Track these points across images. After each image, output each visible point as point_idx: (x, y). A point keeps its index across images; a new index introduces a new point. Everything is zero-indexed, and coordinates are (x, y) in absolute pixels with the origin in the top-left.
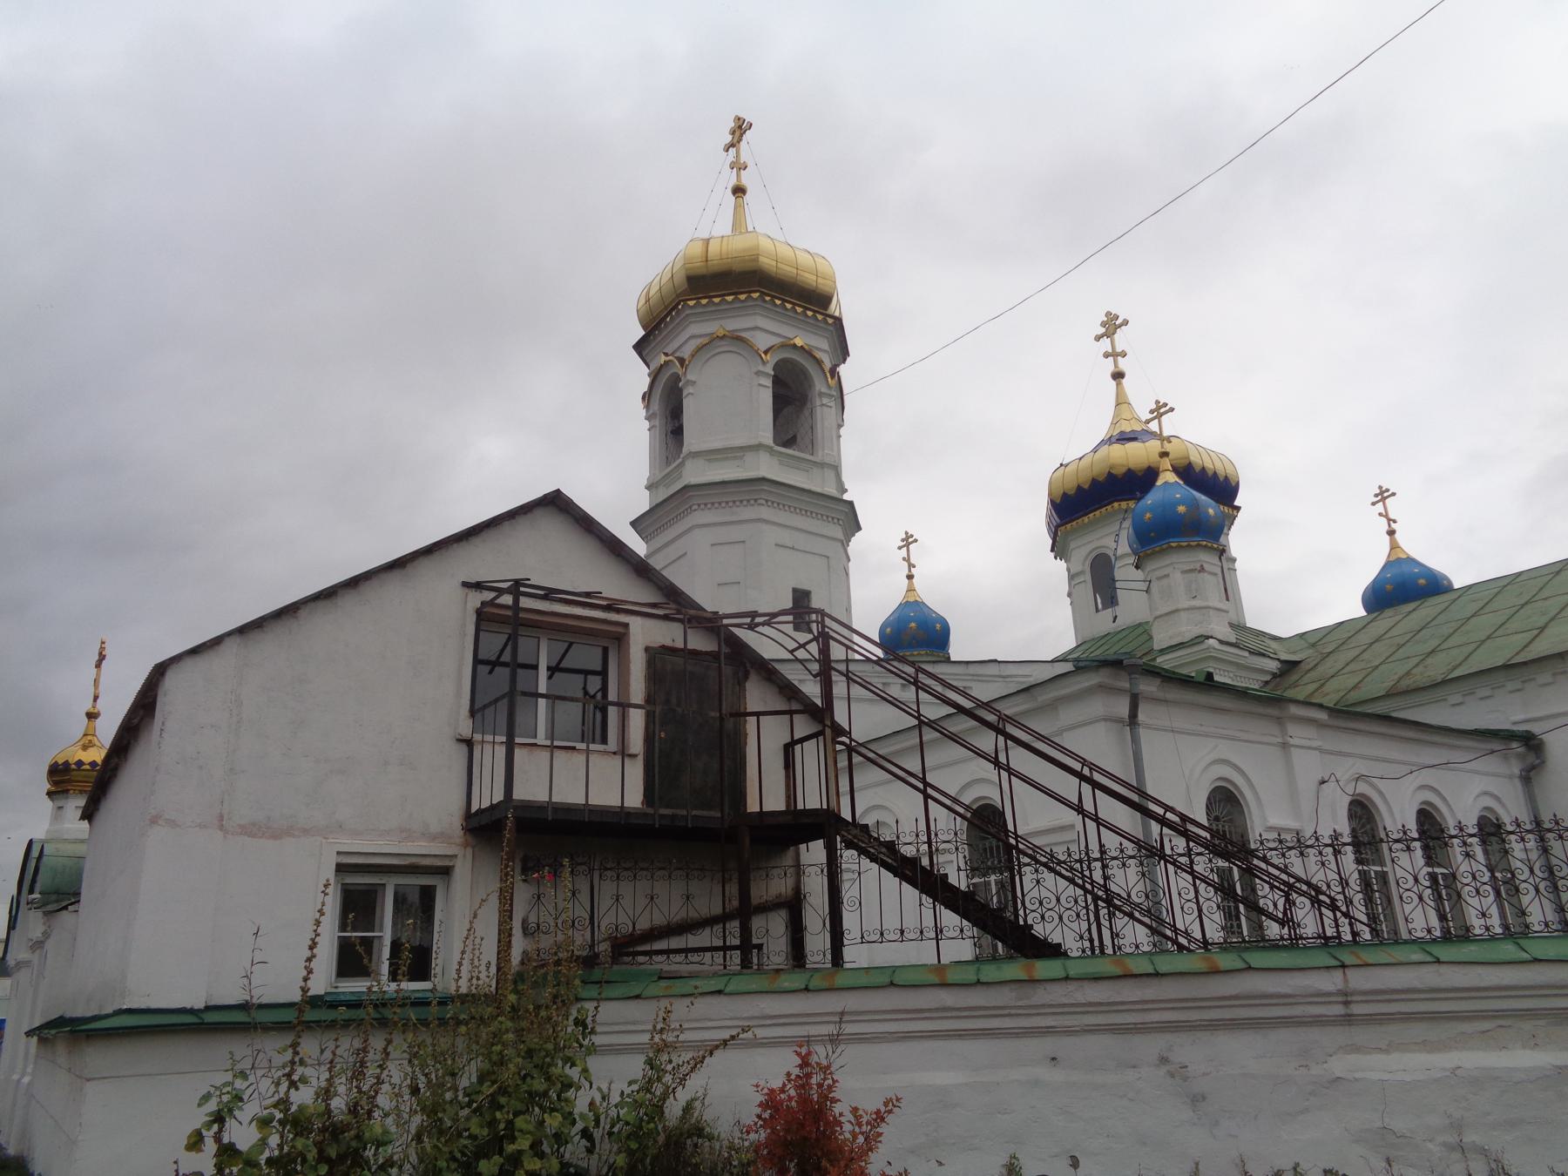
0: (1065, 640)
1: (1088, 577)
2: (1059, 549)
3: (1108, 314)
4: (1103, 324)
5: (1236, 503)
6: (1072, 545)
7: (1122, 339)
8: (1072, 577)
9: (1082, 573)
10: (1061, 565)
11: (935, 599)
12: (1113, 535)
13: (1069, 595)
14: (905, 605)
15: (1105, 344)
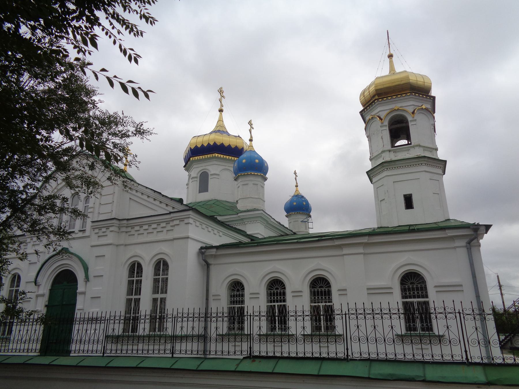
6: (194, 166)
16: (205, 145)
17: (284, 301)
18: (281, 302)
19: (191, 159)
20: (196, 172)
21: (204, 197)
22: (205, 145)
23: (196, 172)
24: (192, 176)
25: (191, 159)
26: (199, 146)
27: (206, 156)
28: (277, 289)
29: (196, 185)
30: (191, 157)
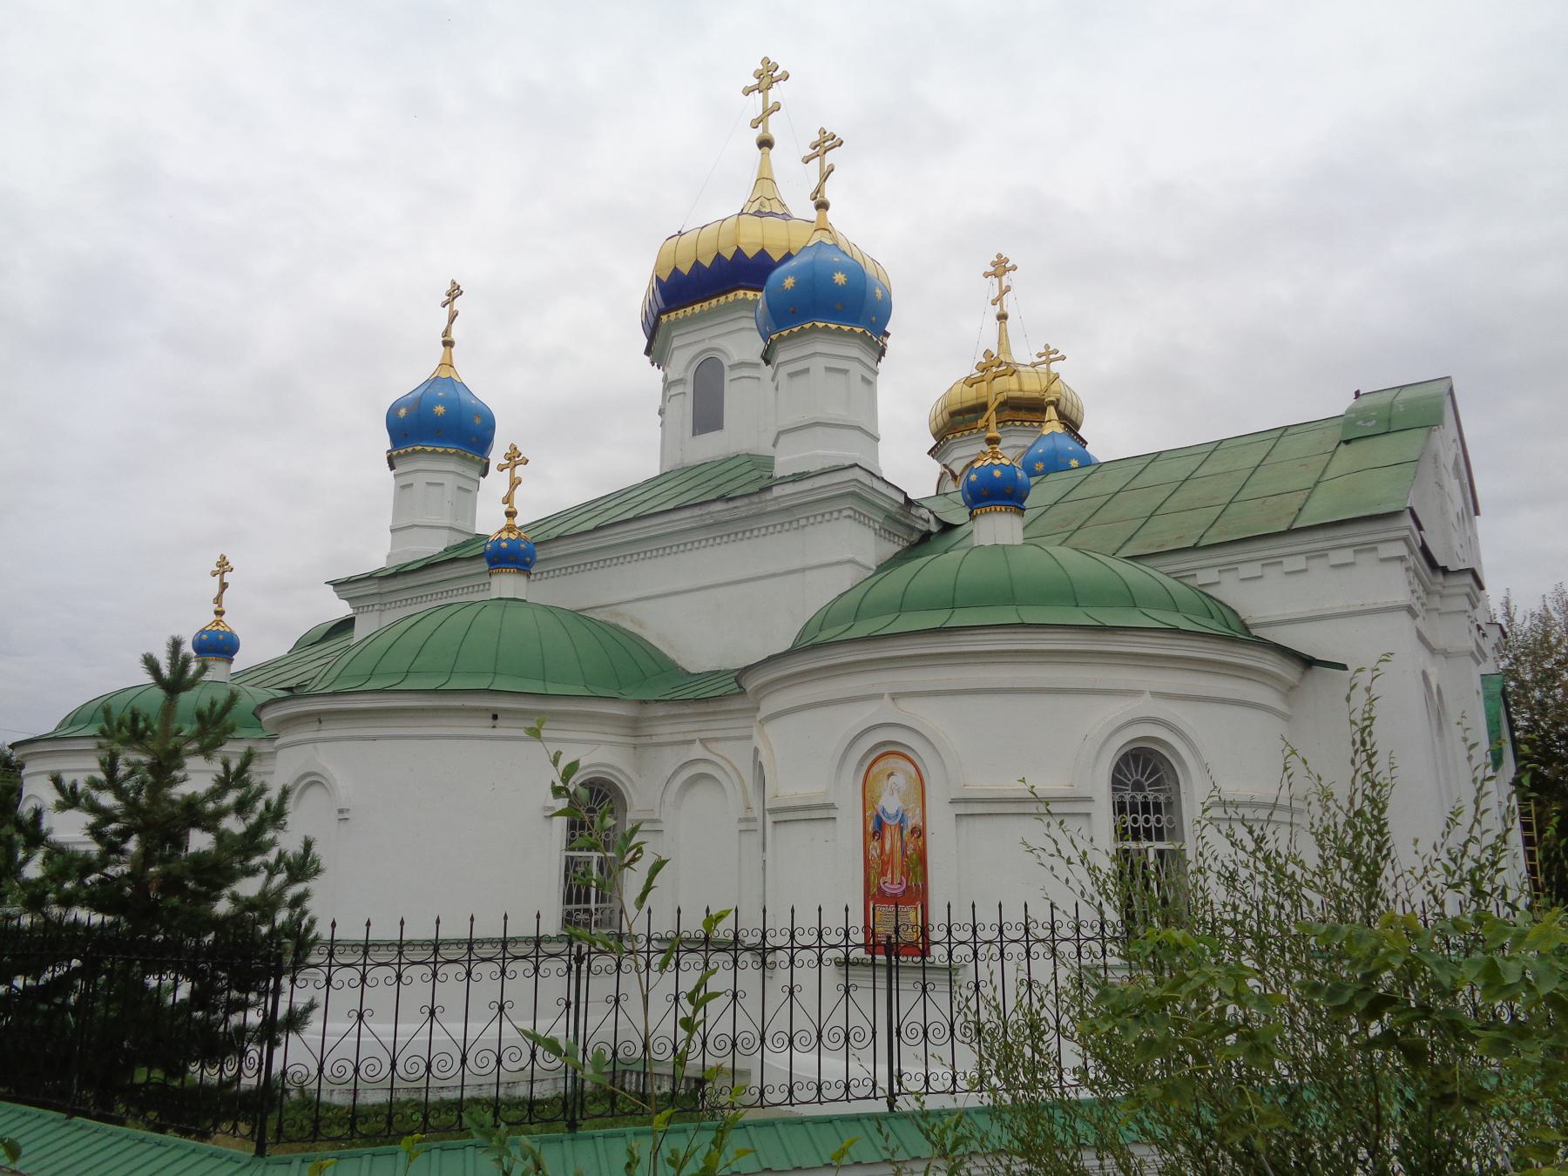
0: (651, 467)
1: (689, 389)
2: (656, 348)
3: (766, 61)
4: (759, 75)
5: (887, 329)
6: (676, 343)
7: (775, 94)
8: (668, 385)
9: (680, 381)
10: (660, 373)
11: (484, 383)
12: (735, 335)
13: (661, 413)
14: (434, 381)
15: (756, 102)
16: (707, 262)
17: (1176, 833)
18: (1160, 838)
19: (664, 318)
20: (683, 358)
21: (711, 447)
22: (707, 262)
23: (683, 358)
24: (670, 378)
25: (664, 318)
26: (685, 269)
27: (689, 310)
28: (1138, 786)
29: (684, 407)
30: (661, 312)
